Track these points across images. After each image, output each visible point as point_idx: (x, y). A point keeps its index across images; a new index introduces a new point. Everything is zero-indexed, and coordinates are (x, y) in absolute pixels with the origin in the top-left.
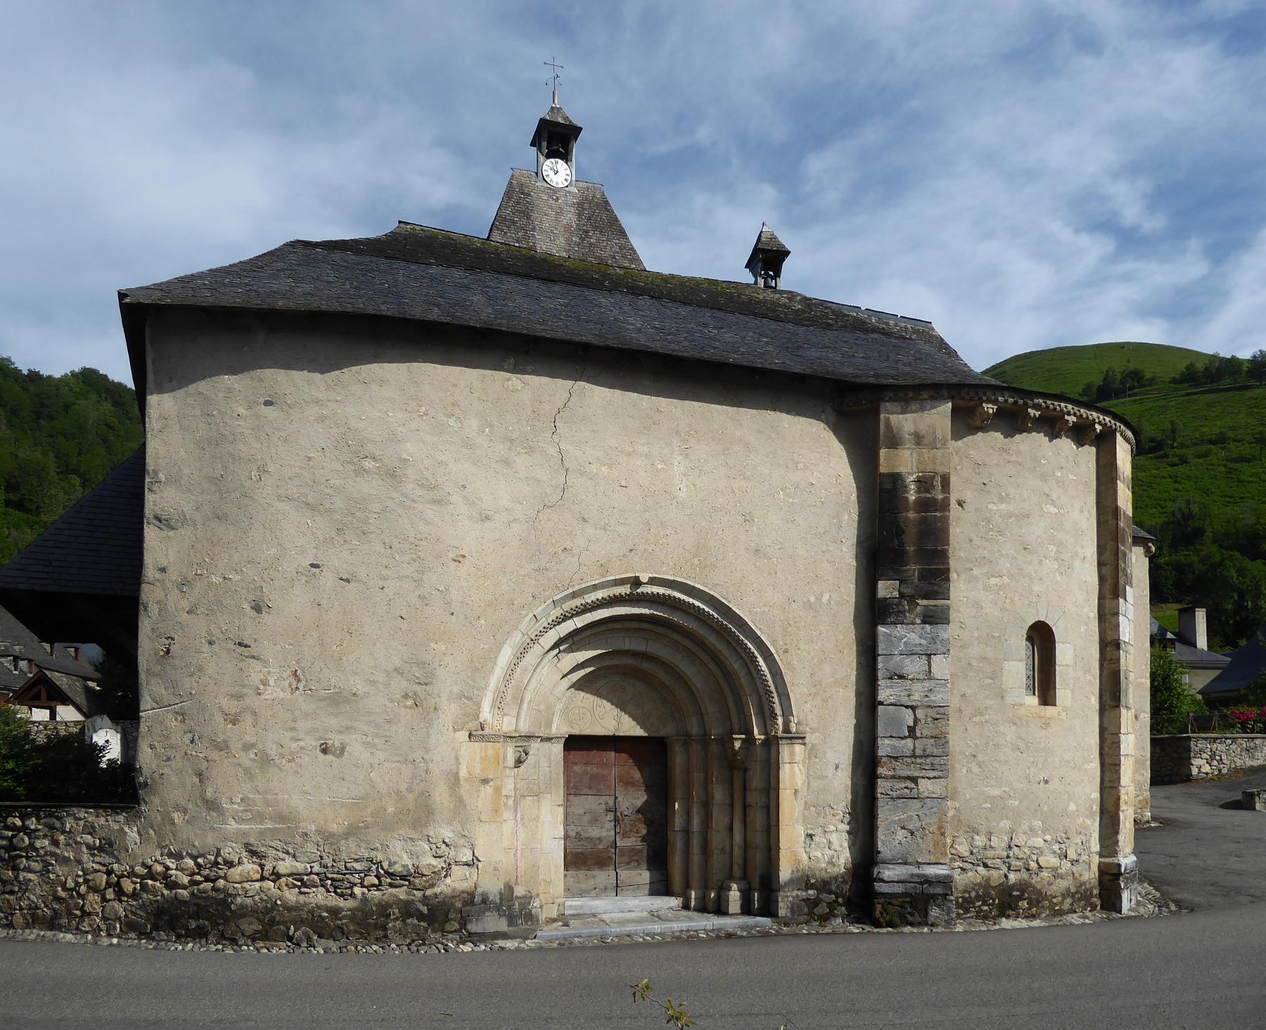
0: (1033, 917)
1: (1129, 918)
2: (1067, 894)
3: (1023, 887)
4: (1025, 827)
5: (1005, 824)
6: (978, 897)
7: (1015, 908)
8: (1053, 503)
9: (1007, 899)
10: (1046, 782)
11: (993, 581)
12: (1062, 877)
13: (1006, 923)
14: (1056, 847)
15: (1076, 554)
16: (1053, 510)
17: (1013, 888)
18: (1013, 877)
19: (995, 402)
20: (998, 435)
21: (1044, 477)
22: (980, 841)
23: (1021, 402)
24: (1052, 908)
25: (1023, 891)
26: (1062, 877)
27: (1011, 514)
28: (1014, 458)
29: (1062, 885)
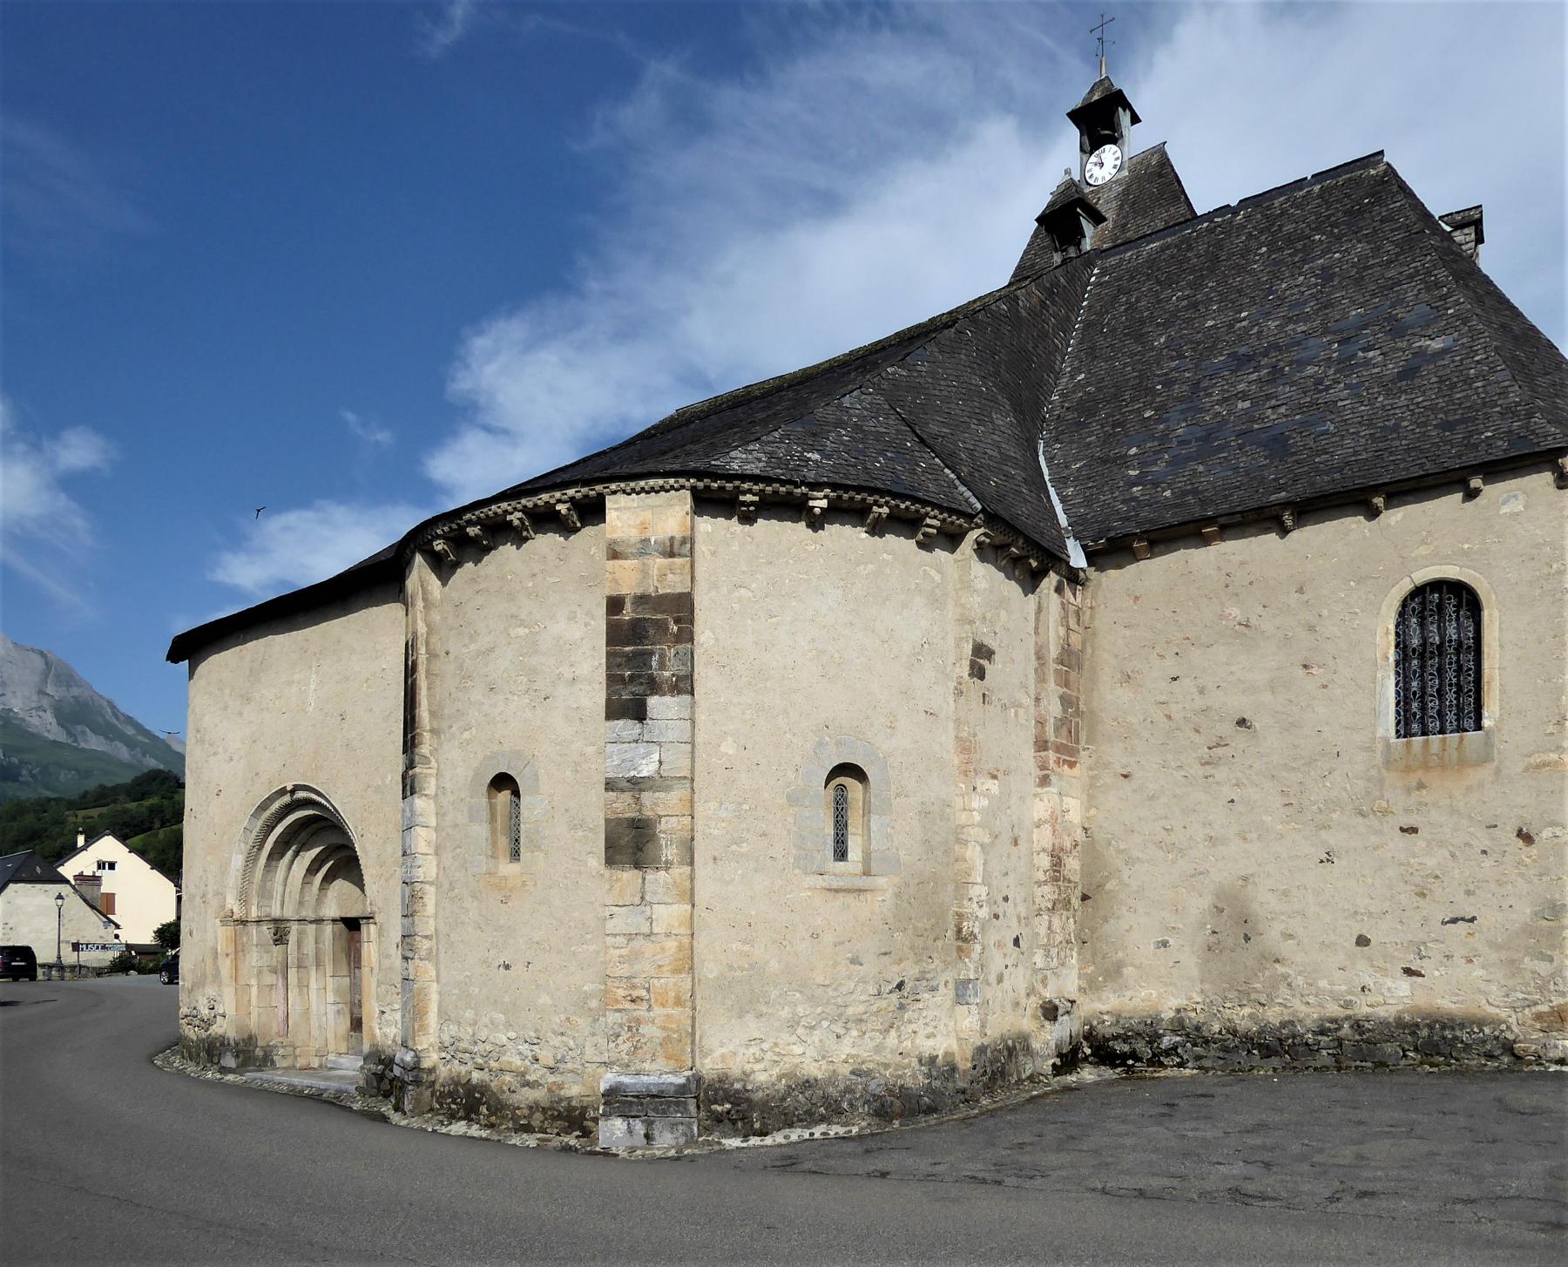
0: (491, 1126)
1: (606, 1153)
2: (534, 1107)
3: (483, 1088)
4: (486, 1020)
5: (469, 1014)
6: (450, 1094)
7: (478, 1113)
8: (522, 624)
9: (469, 1101)
10: (507, 967)
11: (466, 735)
12: (527, 1084)
13: (459, 1128)
14: (524, 1048)
15: (560, 676)
16: (522, 631)
17: (475, 1088)
18: (476, 1076)
19: (438, 537)
20: (471, 565)
21: (511, 597)
22: (453, 1029)
23: (454, 526)
24: (515, 1119)
25: (483, 1095)
26: (527, 1084)
27: (479, 653)
28: (483, 586)
29: (529, 1095)
